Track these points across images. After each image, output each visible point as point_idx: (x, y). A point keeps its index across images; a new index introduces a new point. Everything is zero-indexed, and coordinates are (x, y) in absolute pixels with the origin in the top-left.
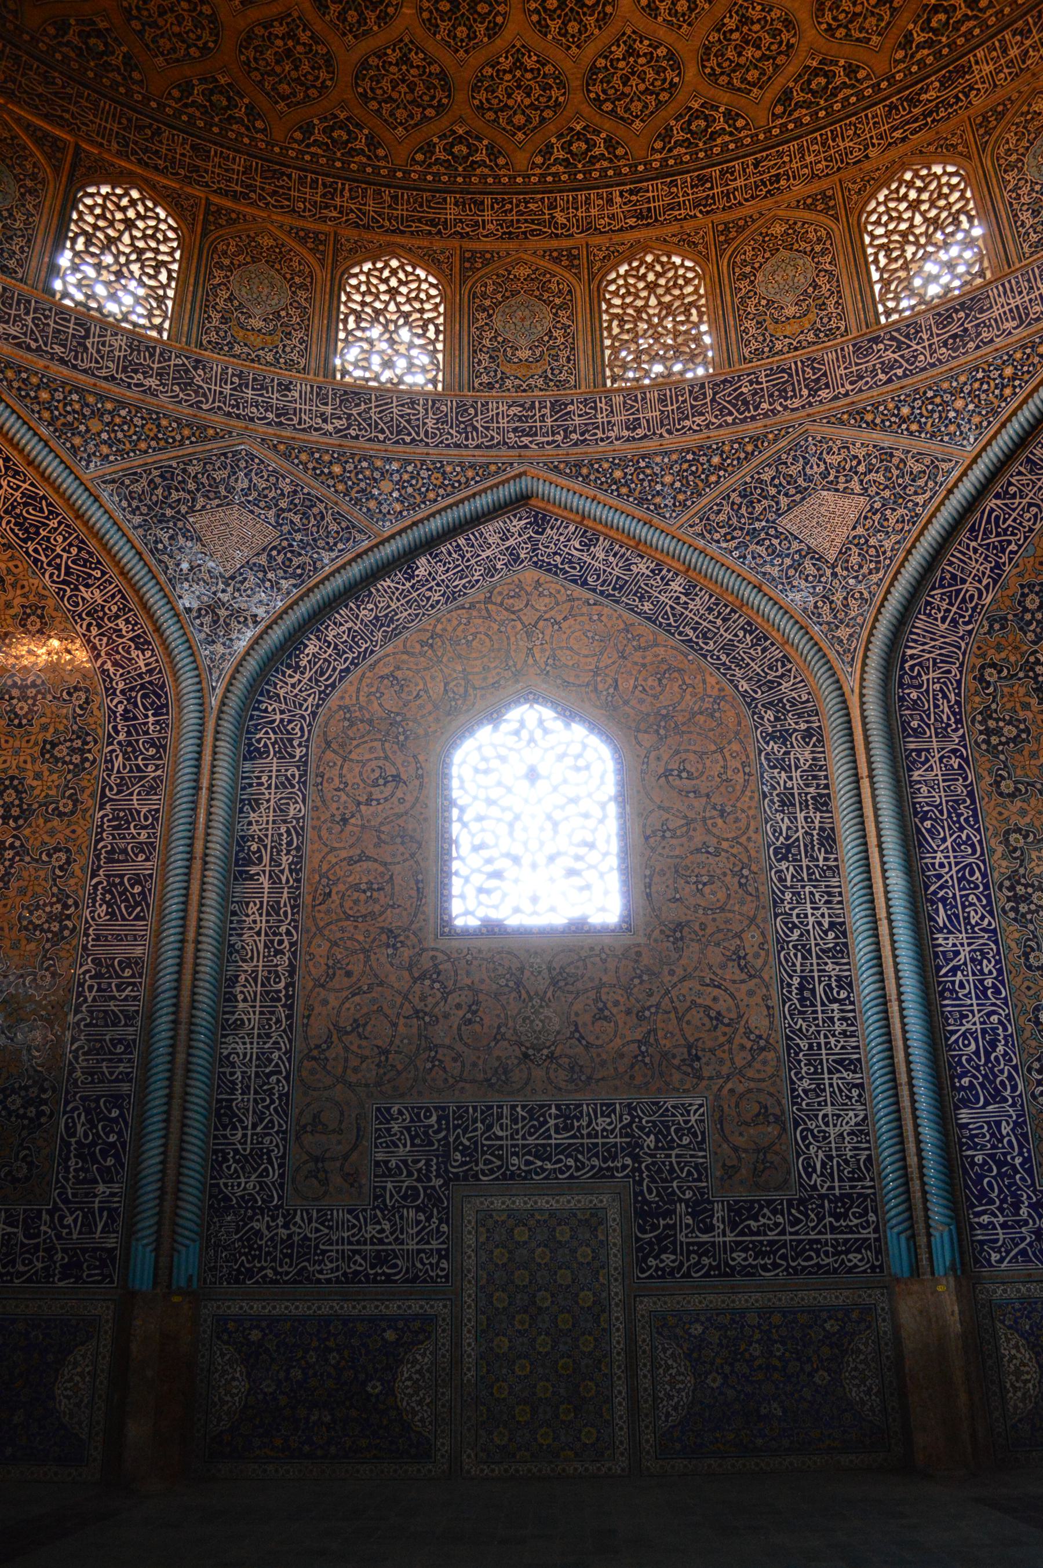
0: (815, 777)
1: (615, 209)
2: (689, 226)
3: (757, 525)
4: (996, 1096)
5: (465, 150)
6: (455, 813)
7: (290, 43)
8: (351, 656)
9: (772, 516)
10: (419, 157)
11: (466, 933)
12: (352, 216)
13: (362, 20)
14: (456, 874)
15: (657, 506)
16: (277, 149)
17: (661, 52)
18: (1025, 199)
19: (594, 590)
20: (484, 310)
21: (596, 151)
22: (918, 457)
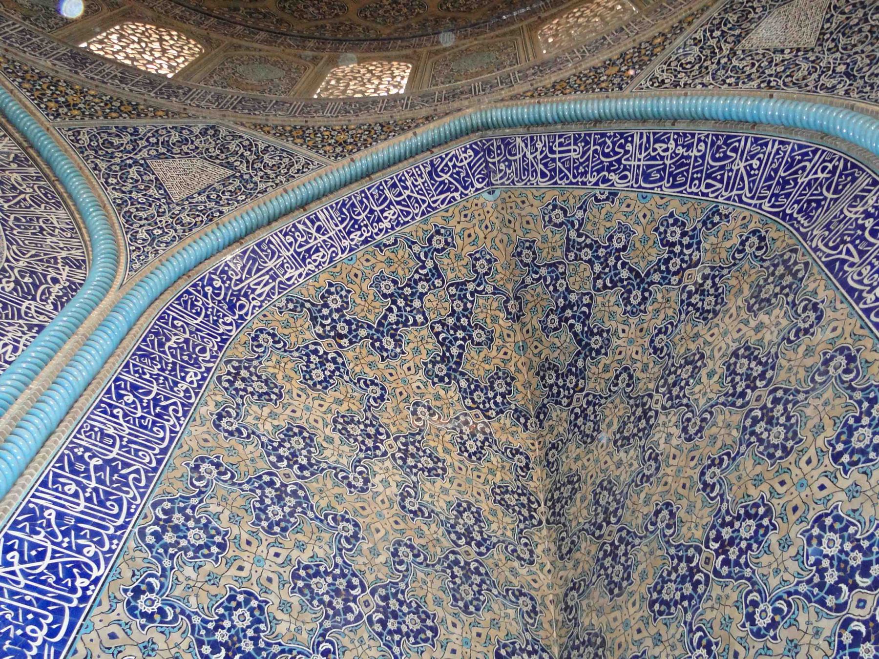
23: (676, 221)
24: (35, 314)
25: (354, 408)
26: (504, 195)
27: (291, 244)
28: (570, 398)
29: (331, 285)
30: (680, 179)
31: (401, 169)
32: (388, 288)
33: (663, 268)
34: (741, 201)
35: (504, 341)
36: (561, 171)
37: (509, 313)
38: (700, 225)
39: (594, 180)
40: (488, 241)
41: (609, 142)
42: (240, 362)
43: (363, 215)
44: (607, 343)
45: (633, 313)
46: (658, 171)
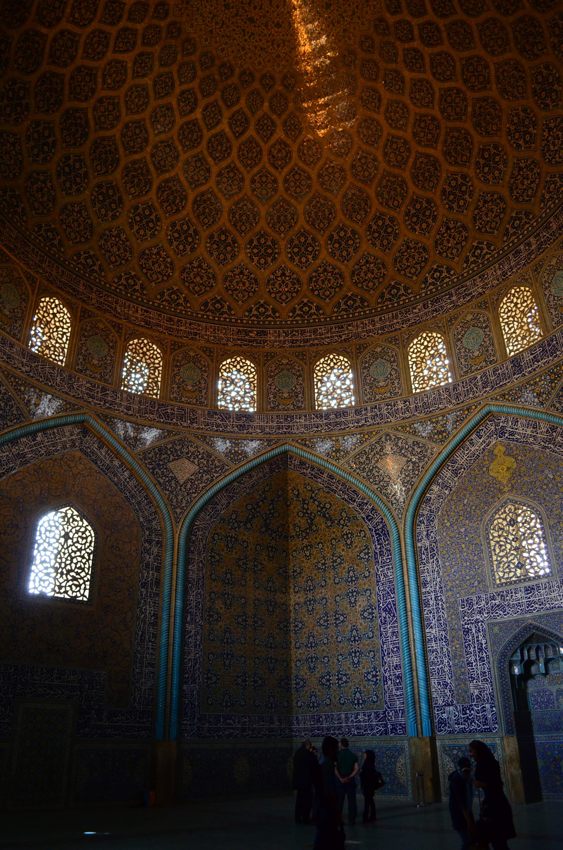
0: (157, 559)
1: (138, 315)
2: (162, 336)
3: (161, 463)
4: (194, 682)
5: (91, 263)
6: (36, 546)
7: (43, 185)
8: (6, 468)
9: (166, 461)
10: (75, 258)
11: (34, 596)
12: (47, 274)
13: (71, 188)
14: (33, 571)
15: (130, 443)
16: (28, 233)
17: (169, 260)
18: (272, 390)
19: (99, 467)
20: (85, 337)
21: (137, 287)
22: (219, 461)
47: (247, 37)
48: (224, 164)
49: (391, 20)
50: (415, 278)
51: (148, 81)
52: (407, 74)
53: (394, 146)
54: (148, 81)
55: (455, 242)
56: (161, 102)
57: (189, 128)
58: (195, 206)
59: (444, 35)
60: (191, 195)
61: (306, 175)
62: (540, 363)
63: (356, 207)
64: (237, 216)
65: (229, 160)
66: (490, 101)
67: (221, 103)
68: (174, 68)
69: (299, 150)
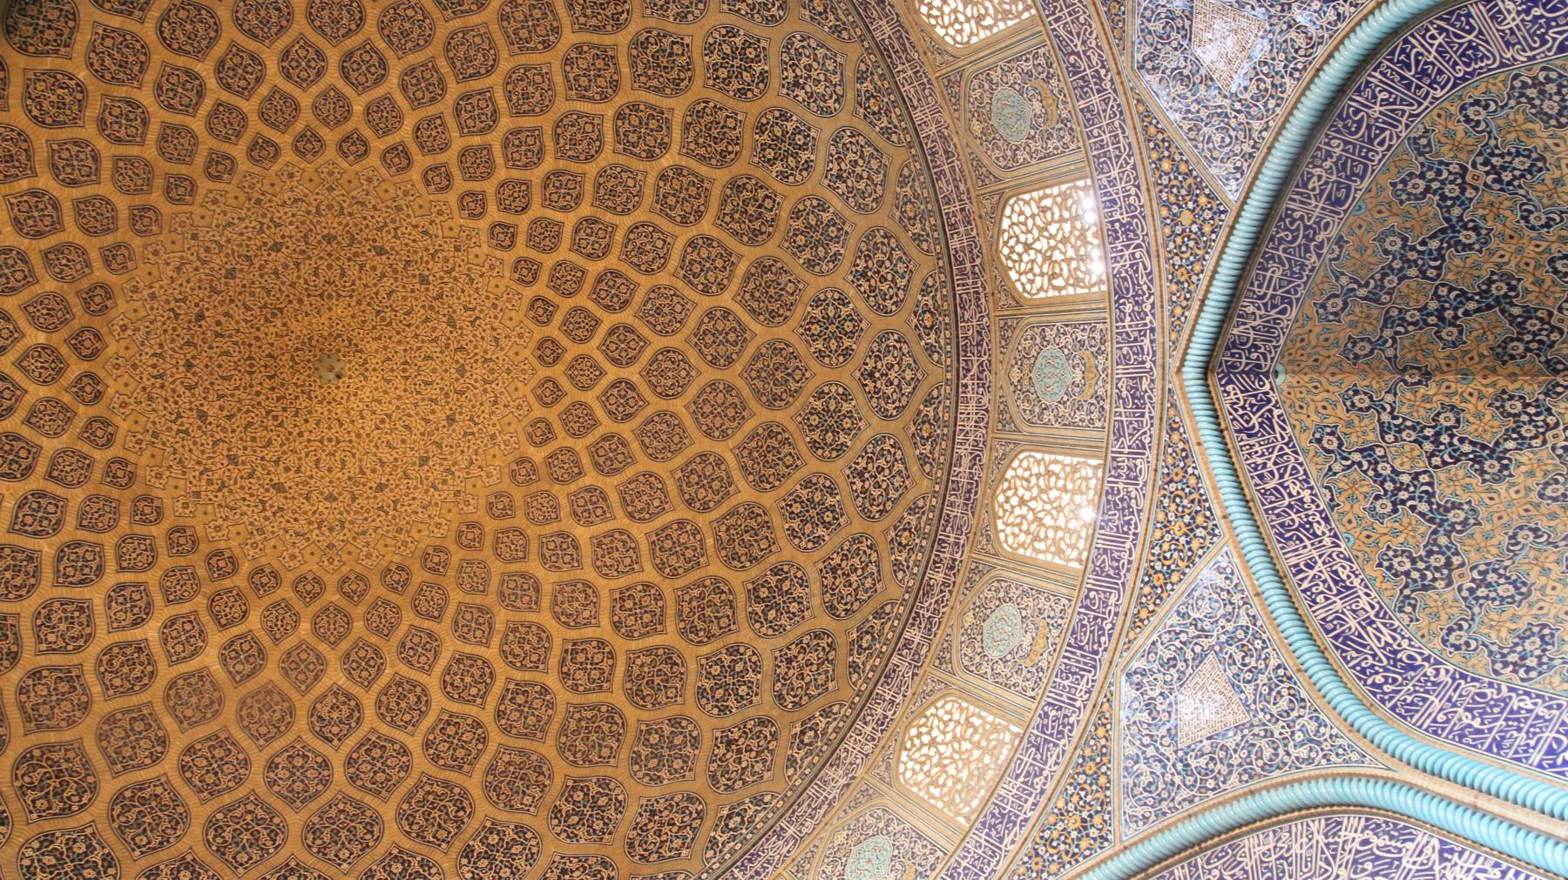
23: (1404, 182)
24: (1423, 857)
25: (1553, 557)
26: (1285, 361)
27: (1327, 599)
28: (1553, 329)
29: (1380, 565)
30: (1359, 169)
31: (1243, 465)
32: (1384, 506)
33: (1449, 203)
34: (1417, 115)
35: (1455, 393)
36: (1288, 292)
37: (1420, 382)
38: (1421, 159)
39: (1314, 257)
40: (1331, 388)
41: (1282, 234)
42: (1494, 662)
43: (1294, 516)
44: (1507, 277)
45: (1485, 243)
46: (1338, 189)
47: (268, 514)
48: (201, 732)
49: (538, 455)
50: (684, 852)
51: (47, 548)
52: (582, 533)
53: (581, 657)
54: (47, 548)
55: (753, 754)
56: (66, 592)
57: (124, 654)
58: (118, 809)
59: (635, 447)
60: (109, 787)
61: (397, 747)
62: (1045, 773)
63: (519, 783)
64: (228, 835)
65: (213, 727)
66: (741, 510)
67: (205, 618)
68: (110, 540)
69: (379, 703)
